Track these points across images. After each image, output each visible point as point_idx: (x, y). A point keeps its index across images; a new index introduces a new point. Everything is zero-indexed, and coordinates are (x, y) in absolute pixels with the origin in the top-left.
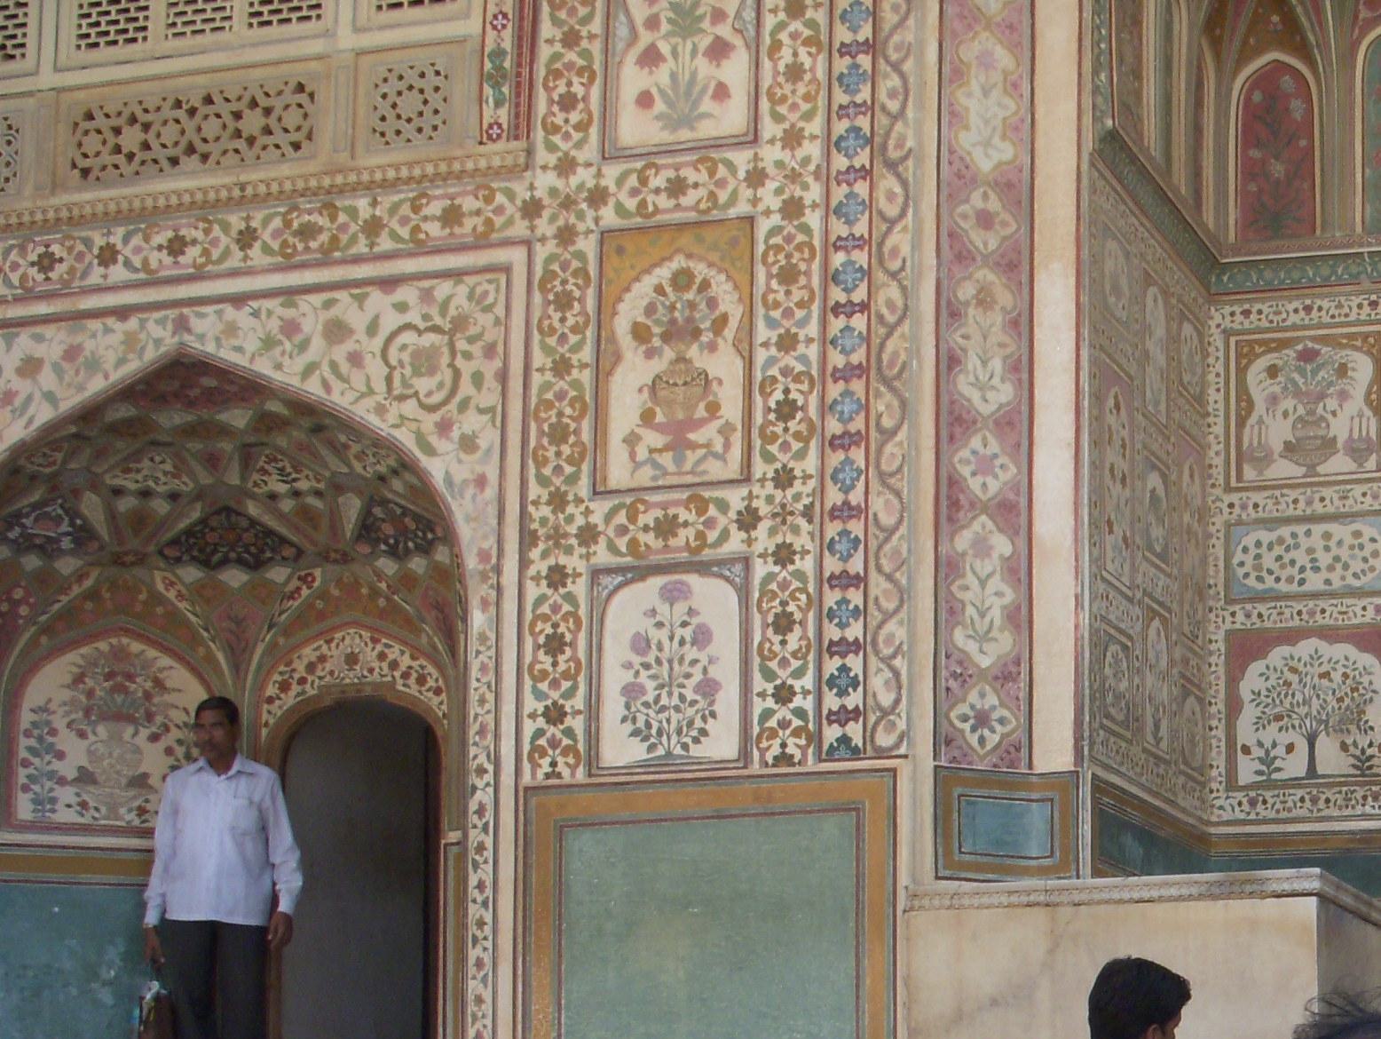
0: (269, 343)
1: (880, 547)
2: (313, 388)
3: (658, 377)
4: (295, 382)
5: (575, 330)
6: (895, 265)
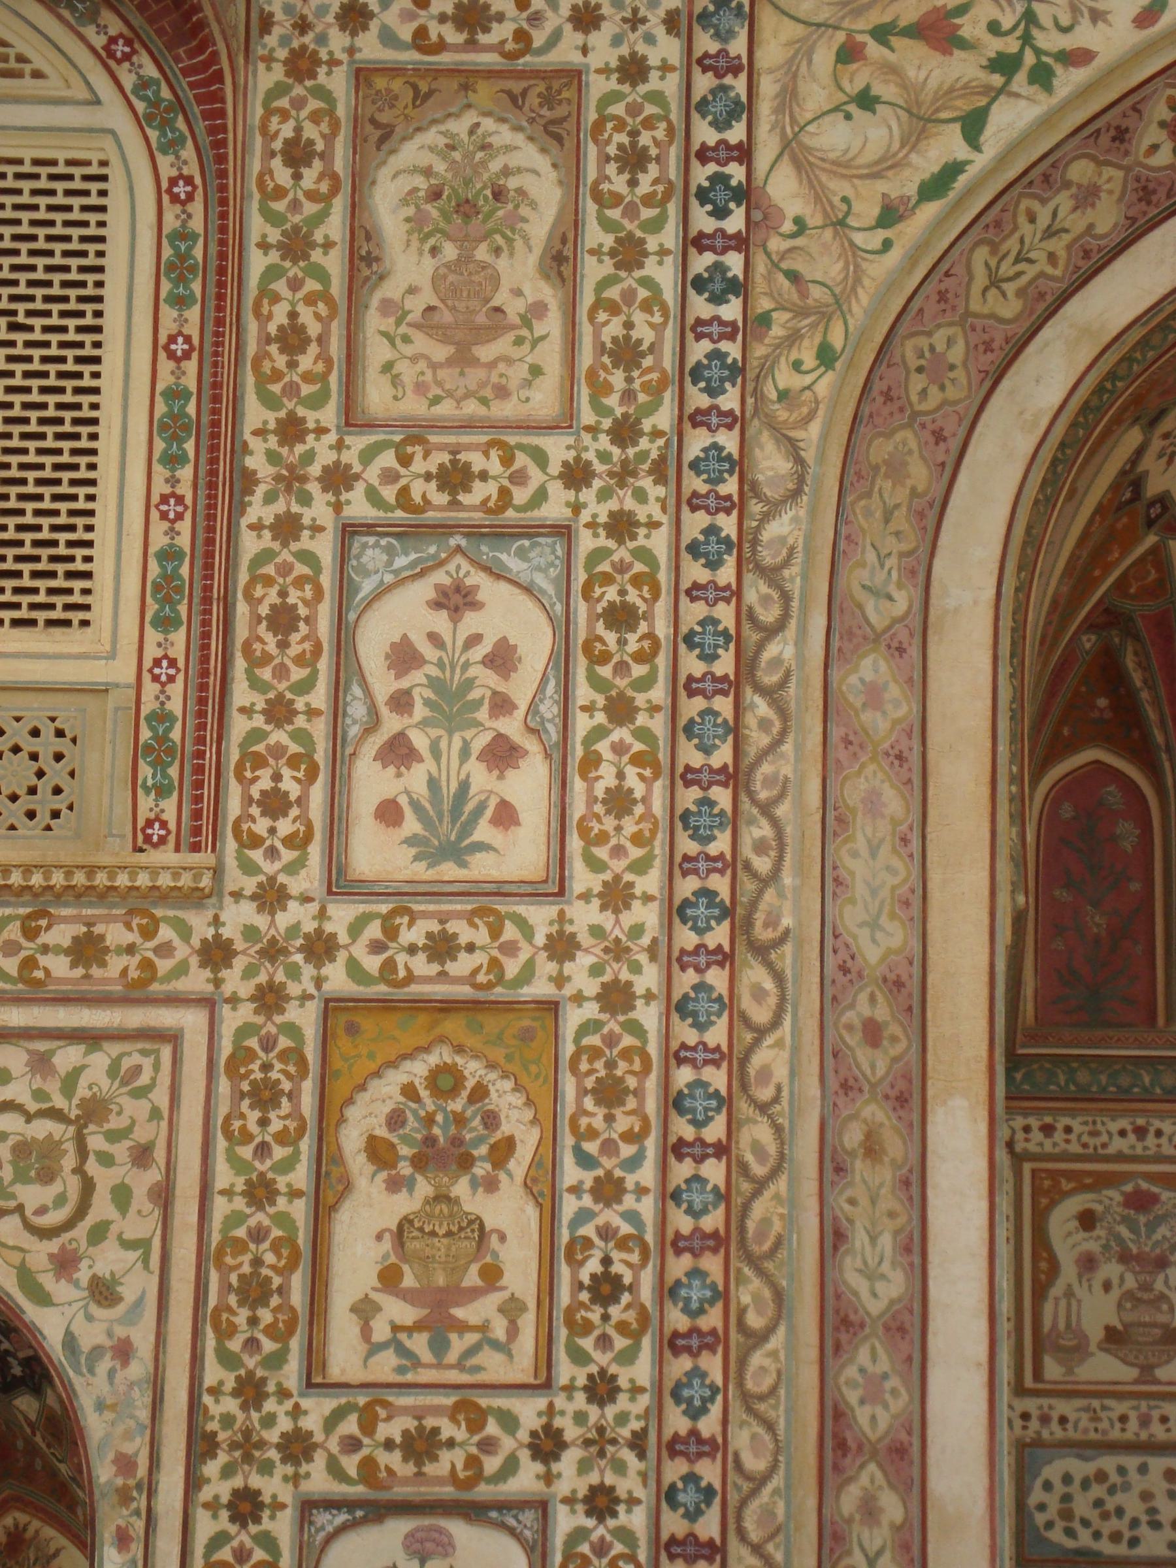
1: (743, 1503)
3: (405, 1223)
5: (282, 1138)
6: (765, 1094)
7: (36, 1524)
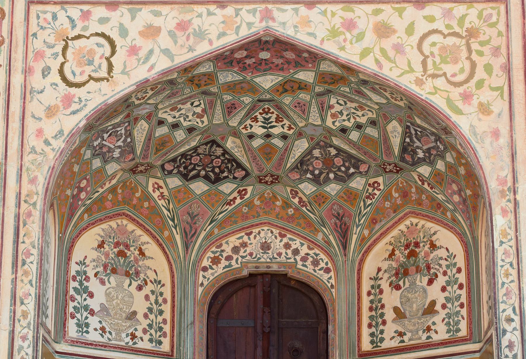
0: (334, 33)
2: (368, 64)
7: (422, 222)
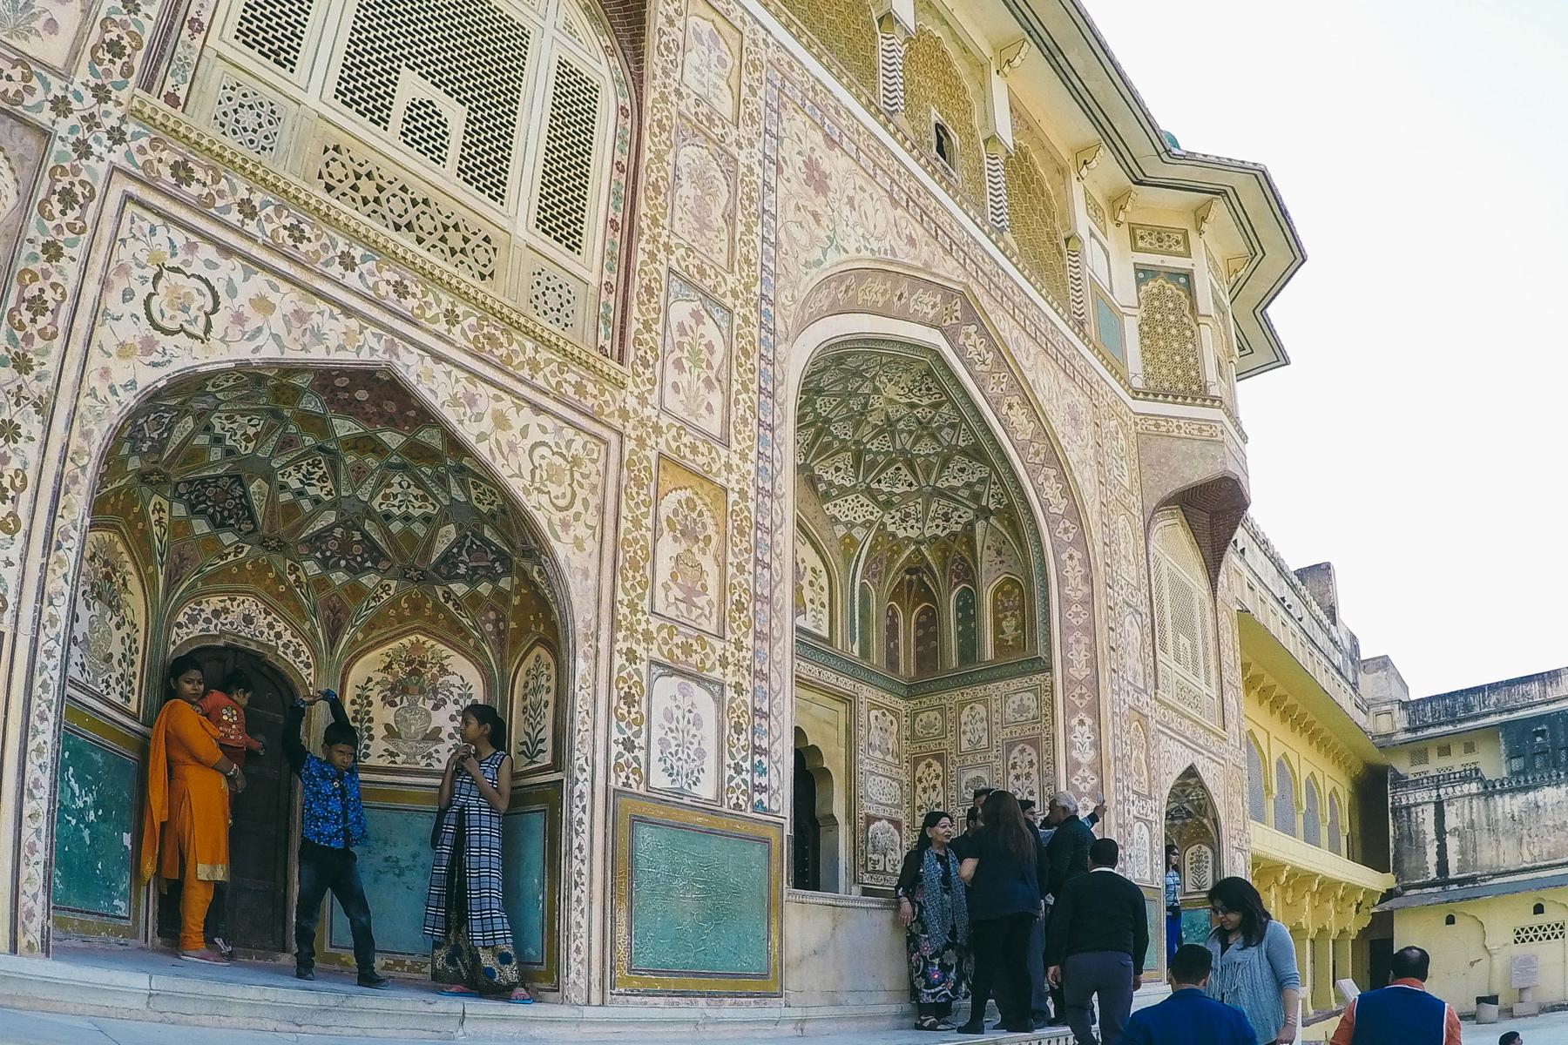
4: (472, 440)
